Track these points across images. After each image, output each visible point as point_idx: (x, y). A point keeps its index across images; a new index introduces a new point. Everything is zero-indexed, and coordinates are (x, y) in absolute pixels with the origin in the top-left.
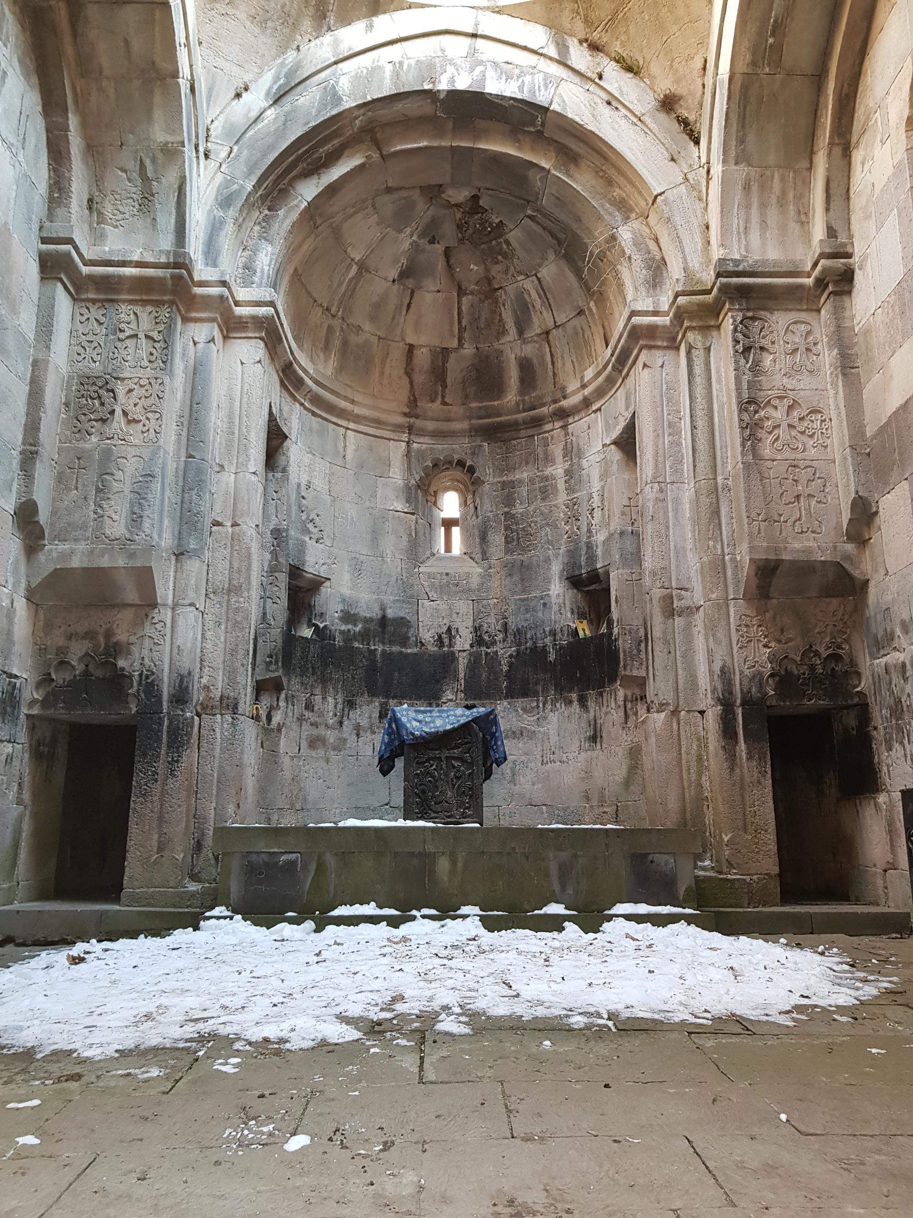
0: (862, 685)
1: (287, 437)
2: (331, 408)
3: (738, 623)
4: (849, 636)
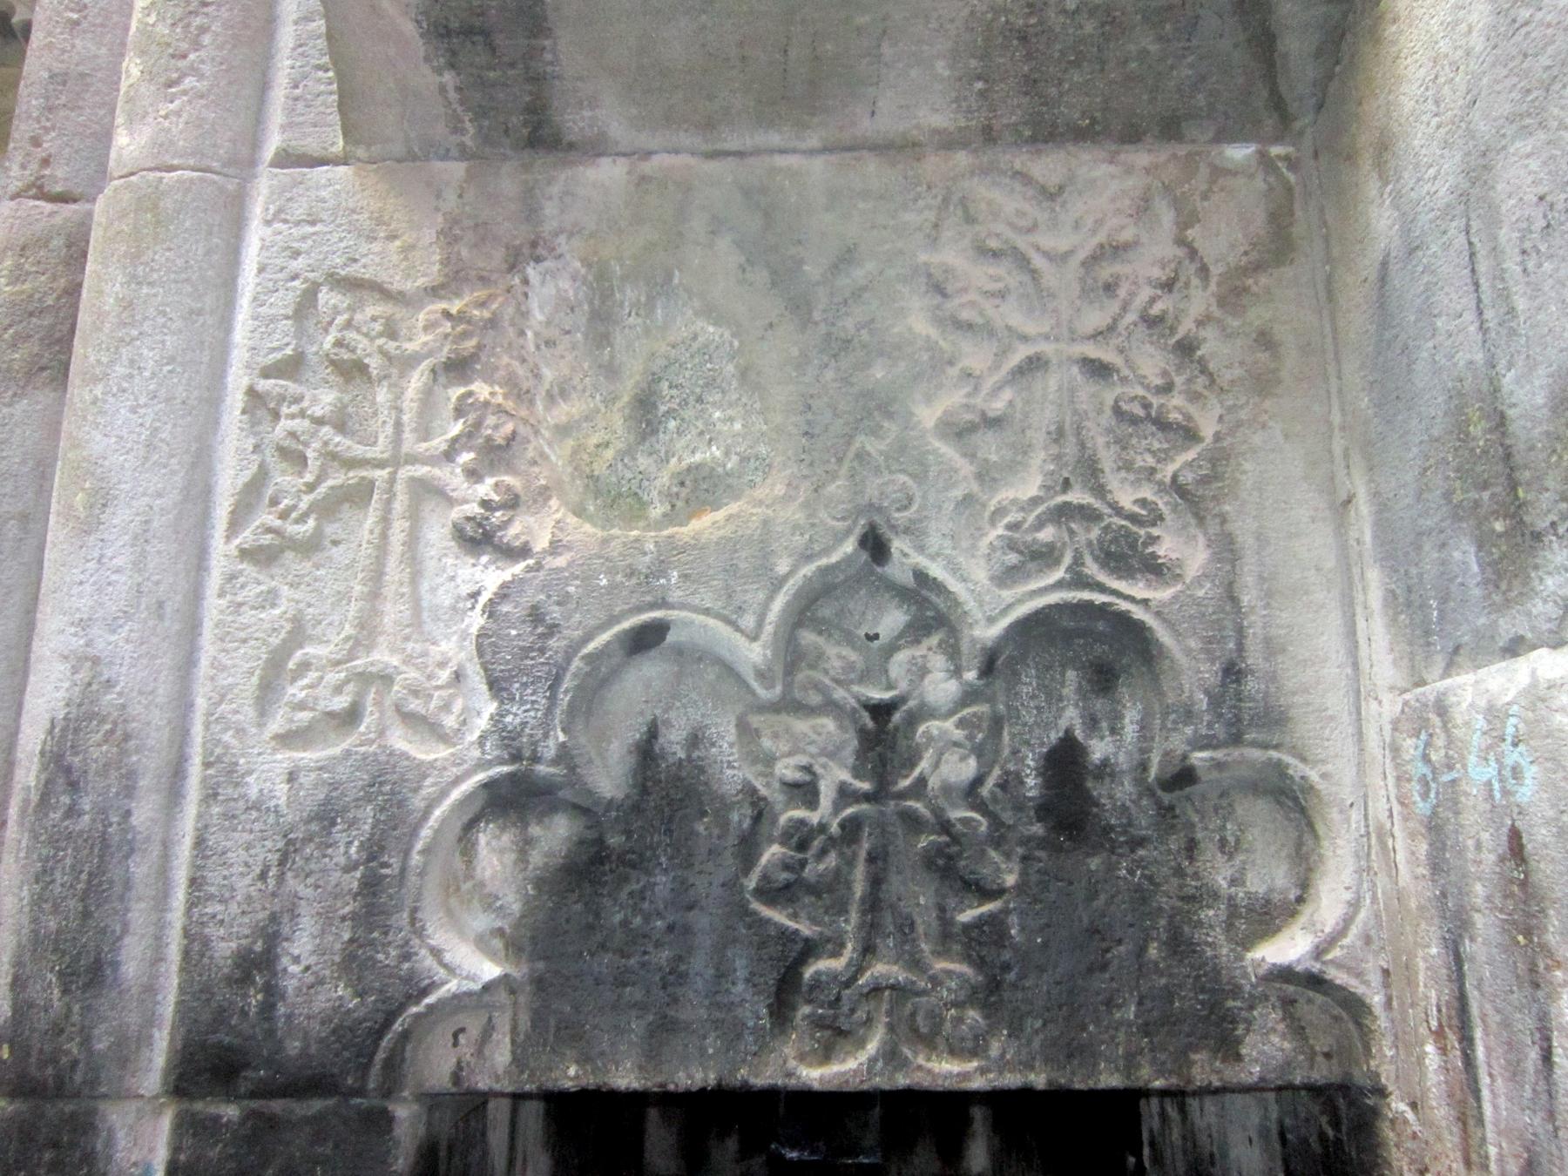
0: (1328, 904)
3: (282, 342)
4: (1219, 461)
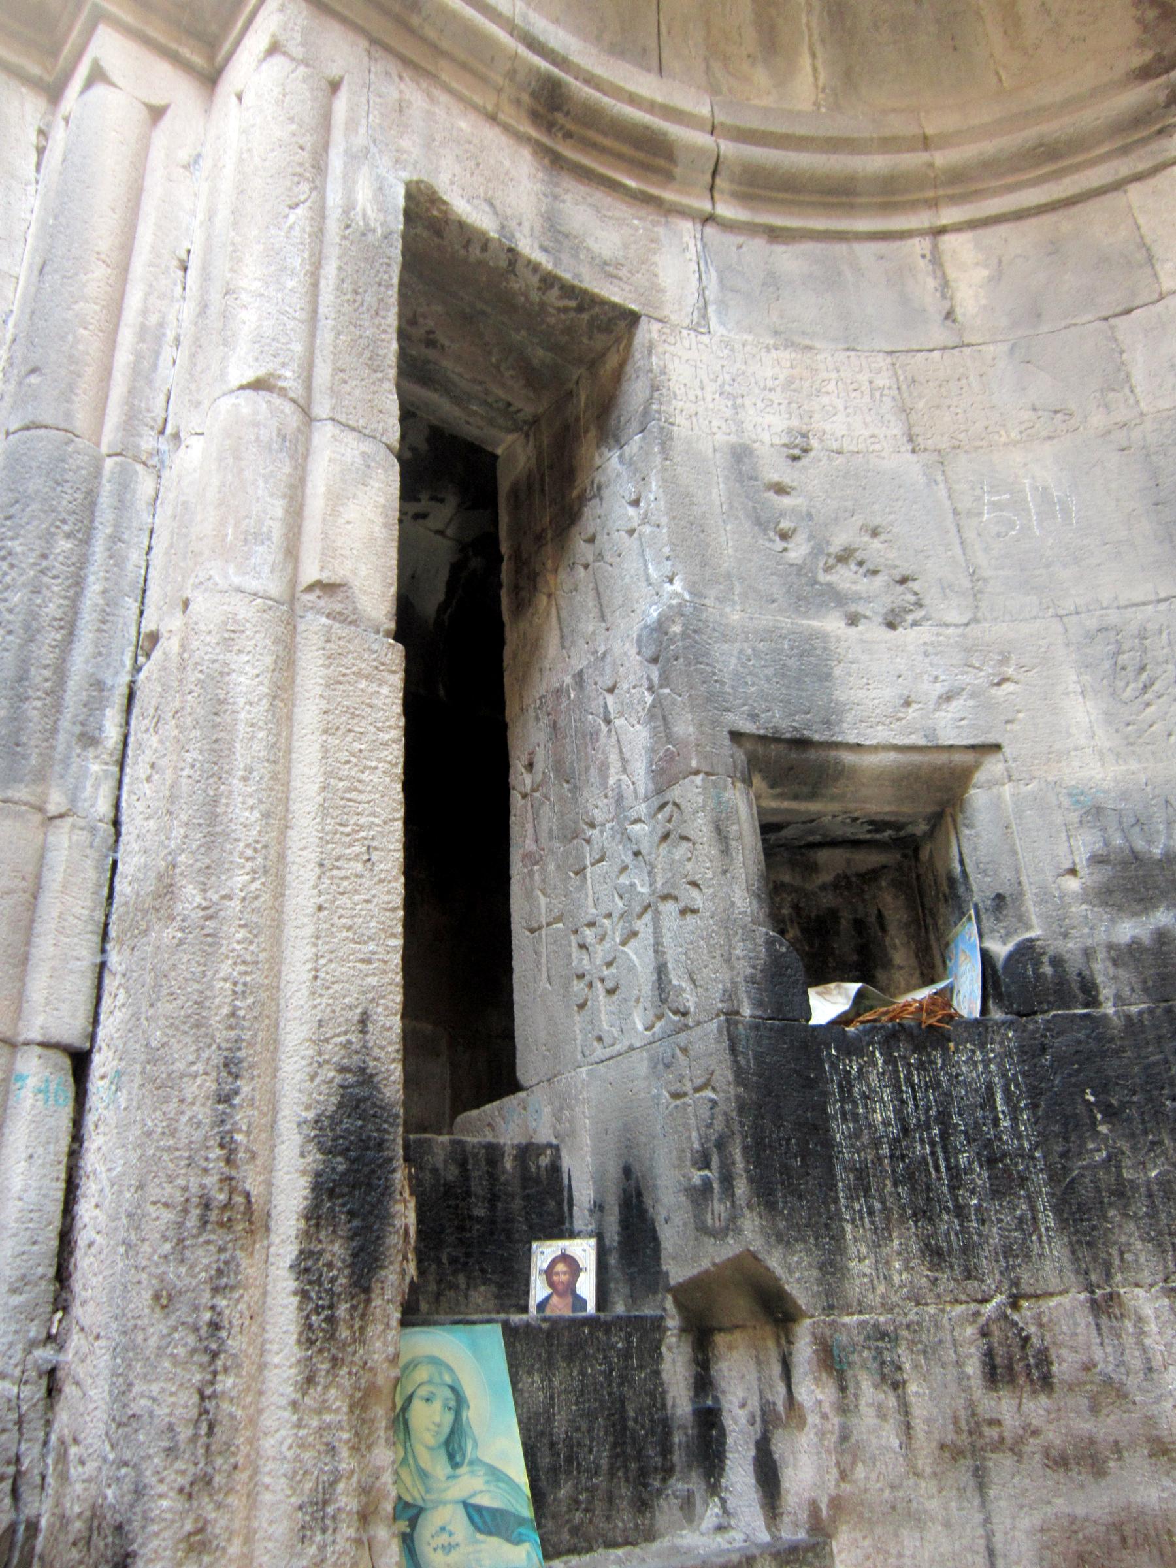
1: (632, 319)
2: (839, 194)
